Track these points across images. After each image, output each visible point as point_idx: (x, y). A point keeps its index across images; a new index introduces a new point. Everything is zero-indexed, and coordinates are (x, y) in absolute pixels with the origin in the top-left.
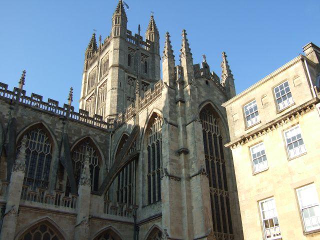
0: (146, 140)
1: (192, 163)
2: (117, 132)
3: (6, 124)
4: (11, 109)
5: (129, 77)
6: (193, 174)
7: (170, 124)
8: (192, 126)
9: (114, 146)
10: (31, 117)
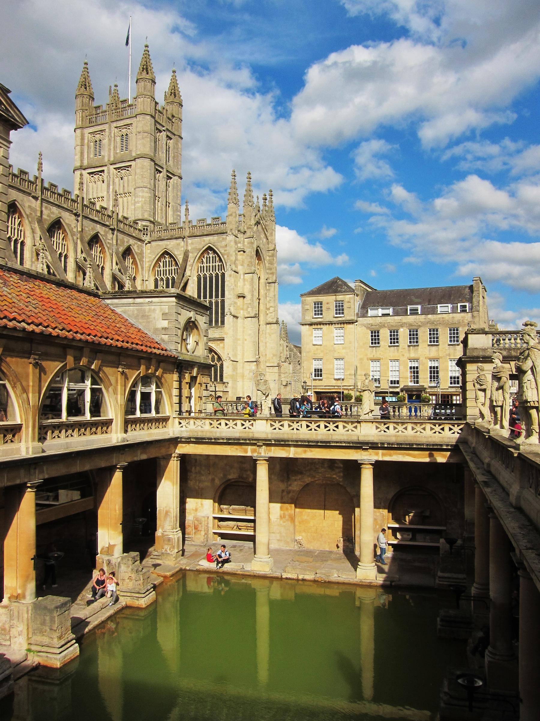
0: (196, 268)
1: (248, 307)
2: (153, 244)
3: (75, 238)
4: (78, 221)
5: (157, 170)
6: (248, 316)
7: (235, 272)
8: (252, 278)
9: (150, 257)
10: (90, 228)
